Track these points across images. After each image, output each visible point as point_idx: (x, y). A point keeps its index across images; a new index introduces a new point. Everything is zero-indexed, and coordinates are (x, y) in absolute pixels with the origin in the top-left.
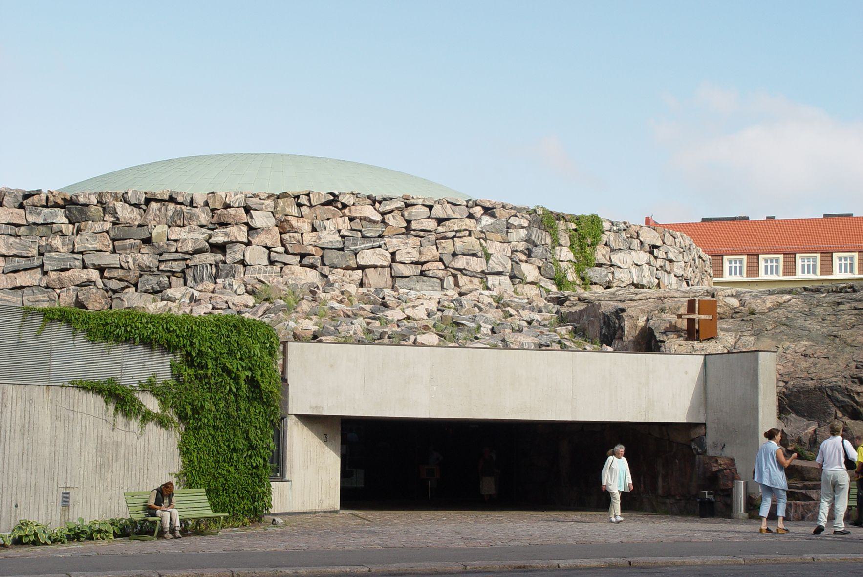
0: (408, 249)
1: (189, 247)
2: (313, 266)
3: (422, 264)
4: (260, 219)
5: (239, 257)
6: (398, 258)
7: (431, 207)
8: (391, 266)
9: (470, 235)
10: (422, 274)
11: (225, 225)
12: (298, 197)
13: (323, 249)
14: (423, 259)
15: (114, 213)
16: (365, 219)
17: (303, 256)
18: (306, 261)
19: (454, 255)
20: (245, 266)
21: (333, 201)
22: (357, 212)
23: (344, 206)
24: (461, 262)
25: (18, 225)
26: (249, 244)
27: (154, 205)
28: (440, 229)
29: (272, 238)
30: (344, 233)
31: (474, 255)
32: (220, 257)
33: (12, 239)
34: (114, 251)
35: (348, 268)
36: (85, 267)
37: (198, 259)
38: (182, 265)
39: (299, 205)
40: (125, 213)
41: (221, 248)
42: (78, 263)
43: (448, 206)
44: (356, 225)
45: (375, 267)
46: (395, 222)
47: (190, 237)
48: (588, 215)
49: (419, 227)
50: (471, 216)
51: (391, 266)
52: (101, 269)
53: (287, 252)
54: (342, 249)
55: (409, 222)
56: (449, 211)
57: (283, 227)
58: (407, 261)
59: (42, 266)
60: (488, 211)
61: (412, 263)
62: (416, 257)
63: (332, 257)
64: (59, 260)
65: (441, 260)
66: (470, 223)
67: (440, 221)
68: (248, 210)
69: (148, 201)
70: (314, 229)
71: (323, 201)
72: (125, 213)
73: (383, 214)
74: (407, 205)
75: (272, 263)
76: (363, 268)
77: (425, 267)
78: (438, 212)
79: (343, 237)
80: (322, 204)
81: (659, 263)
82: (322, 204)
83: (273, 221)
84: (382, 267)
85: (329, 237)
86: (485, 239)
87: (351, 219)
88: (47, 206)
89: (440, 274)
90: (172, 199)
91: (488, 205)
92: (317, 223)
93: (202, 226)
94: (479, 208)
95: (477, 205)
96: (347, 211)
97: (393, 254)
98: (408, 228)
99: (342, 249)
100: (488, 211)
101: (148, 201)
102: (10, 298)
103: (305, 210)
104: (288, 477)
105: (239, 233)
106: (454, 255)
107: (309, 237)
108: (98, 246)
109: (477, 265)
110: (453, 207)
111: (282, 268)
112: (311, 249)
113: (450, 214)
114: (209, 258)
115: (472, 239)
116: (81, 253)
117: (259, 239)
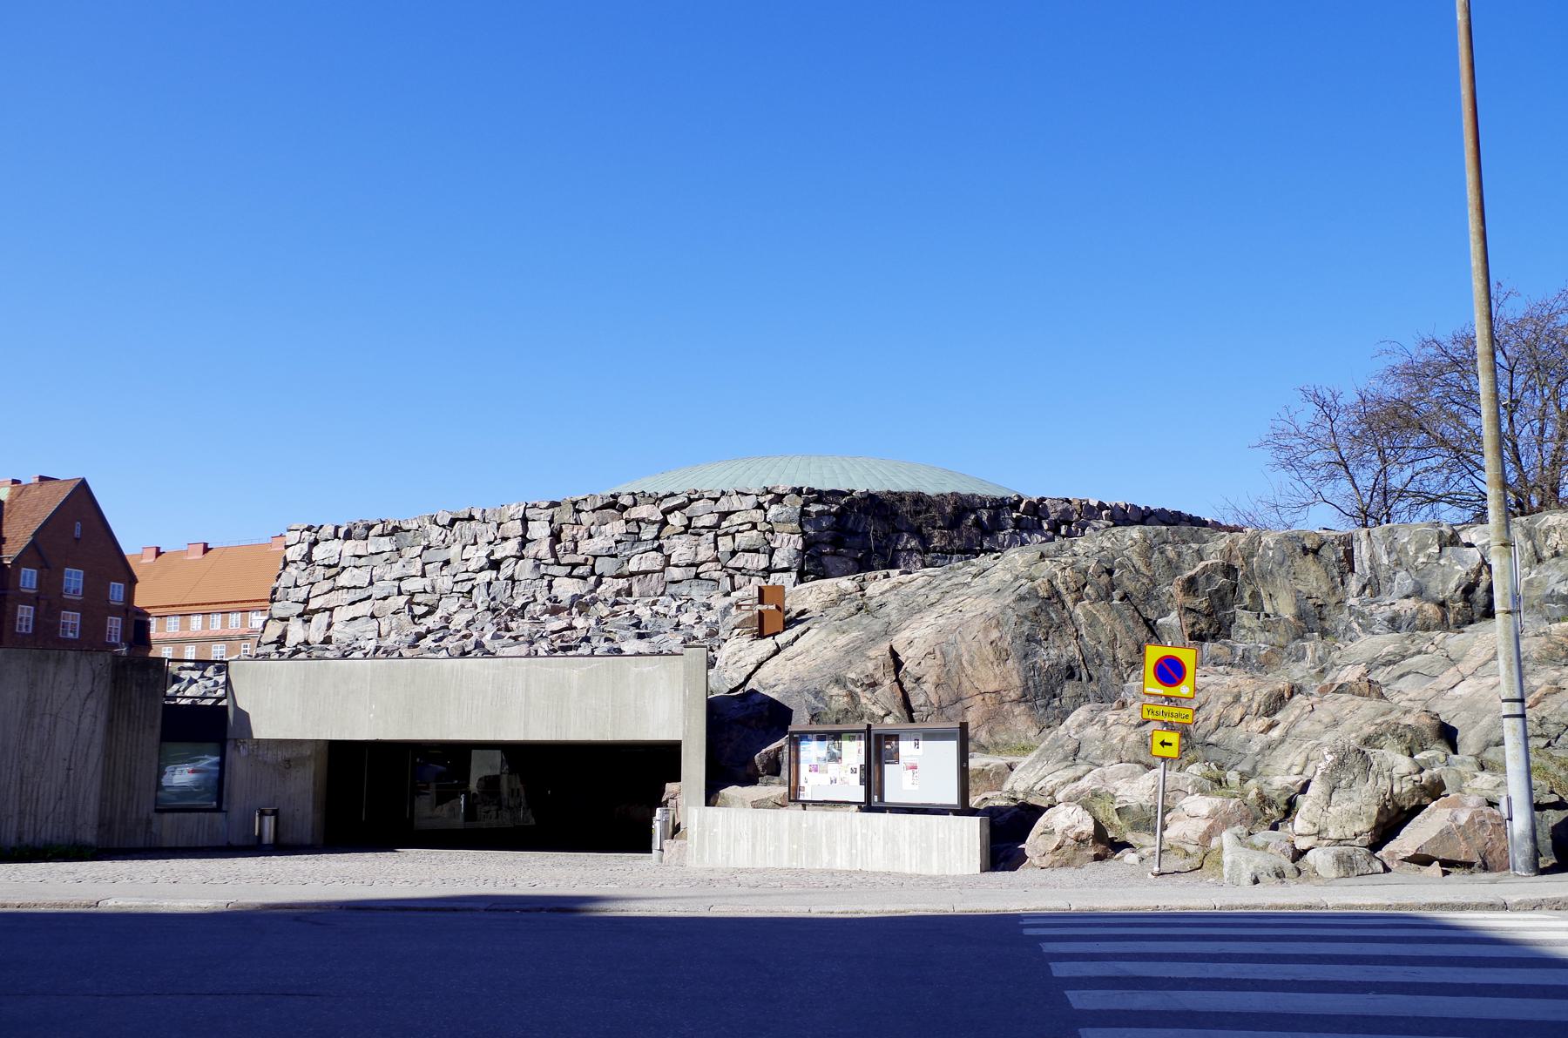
0: (680, 549)
1: (473, 566)
3: (697, 566)
6: (673, 560)
7: (716, 500)
8: (663, 571)
10: (697, 576)
11: (505, 539)
12: (575, 504)
13: (595, 557)
14: (700, 558)
15: (426, 537)
16: (643, 520)
17: (574, 566)
18: (575, 573)
19: (734, 553)
20: (514, 582)
21: (613, 504)
22: (635, 513)
23: (625, 508)
24: (740, 561)
25: (360, 557)
26: (522, 557)
28: (724, 524)
29: (544, 550)
31: (757, 551)
34: (424, 575)
35: (617, 577)
36: (400, 593)
38: (467, 586)
39: (578, 511)
41: (495, 565)
43: (735, 497)
44: (633, 528)
45: (646, 573)
46: (676, 520)
47: (478, 556)
48: (931, 490)
49: (700, 524)
50: (760, 506)
51: (663, 571)
54: (615, 556)
55: (690, 519)
56: (735, 502)
57: (556, 537)
58: (683, 563)
60: (779, 499)
61: (688, 565)
62: (689, 557)
65: (717, 560)
66: (757, 515)
67: (724, 515)
68: (525, 520)
69: (453, 522)
70: (590, 536)
71: (599, 504)
72: (435, 534)
73: (666, 512)
74: (691, 501)
75: (542, 577)
76: (632, 574)
78: (723, 505)
79: (617, 542)
80: (601, 508)
82: (601, 508)
83: (548, 532)
84: (654, 572)
85: (598, 544)
86: (772, 532)
87: (627, 522)
88: (382, 535)
89: (716, 575)
90: (471, 518)
92: (593, 528)
93: (490, 543)
94: (770, 497)
95: (768, 492)
96: (625, 515)
98: (687, 527)
99: (615, 556)
100: (779, 499)
101: (453, 522)
102: (347, 630)
103: (583, 515)
104: (224, 807)
105: (511, 547)
106: (734, 553)
110: (743, 498)
111: (550, 583)
112: (580, 559)
113: (736, 505)
116: (400, 579)
117: (531, 550)
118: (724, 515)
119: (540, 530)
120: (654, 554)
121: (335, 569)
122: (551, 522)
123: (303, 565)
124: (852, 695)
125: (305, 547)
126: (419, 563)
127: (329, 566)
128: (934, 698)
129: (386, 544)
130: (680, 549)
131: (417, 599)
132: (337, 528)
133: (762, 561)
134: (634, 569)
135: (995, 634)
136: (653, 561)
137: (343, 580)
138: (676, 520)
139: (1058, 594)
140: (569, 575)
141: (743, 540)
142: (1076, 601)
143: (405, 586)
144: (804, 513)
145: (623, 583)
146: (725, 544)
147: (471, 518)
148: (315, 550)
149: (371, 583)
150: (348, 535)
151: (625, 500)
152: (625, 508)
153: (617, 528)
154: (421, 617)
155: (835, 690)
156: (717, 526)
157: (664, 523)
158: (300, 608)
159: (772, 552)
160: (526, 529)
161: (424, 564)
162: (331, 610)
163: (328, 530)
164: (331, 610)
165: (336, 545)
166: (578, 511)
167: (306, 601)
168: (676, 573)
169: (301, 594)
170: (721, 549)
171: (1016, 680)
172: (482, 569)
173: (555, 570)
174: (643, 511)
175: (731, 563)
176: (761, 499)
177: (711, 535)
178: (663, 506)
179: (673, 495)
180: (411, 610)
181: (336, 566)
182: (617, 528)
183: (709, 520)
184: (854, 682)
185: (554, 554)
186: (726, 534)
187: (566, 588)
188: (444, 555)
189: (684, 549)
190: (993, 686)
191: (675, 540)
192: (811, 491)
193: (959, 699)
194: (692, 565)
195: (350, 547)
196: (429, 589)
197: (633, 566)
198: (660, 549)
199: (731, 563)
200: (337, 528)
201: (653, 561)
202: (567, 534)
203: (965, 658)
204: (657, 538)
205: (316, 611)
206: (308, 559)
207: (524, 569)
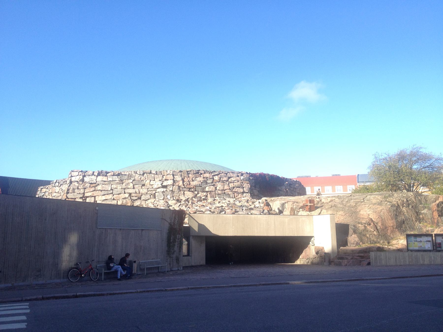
0: (219, 186)
2: (192, 192)
4: (178, 178)
5: (171, 189)
6: (218, 188)
7: (227, 174)
9: (238, 182)
10: (225, 193)
12: (187, 172)
14: (225, 188)
17: (190, 188)
18: (190, 190)
19: (234, 188)
23: (201, 174)
24: (236, 190)
25: (105, 181)
27: (145, 174)
28: (230, 180)
29: (181, 183)
30: (202, 182)
32: (165, 189)
33: (103, 186)
34: (134, 188)
36: (125, 193)
37: (158, 190)
38: (154, 192)
40: (137, 177)
41: (165, 187)
42: (123, 192)
45: (211, 191)
49: (223, 180)
50: (238, 176)
52: (130, 194)
53: (185, 187)
55: (220, 178)
56: (232, 175)
58: (220, 189)
59: (112, 193)
60: (242, 175)
62: (222, 188)
63: (199, 189)
64: (117, 191)
65: (230, 189)
66: (238, 178)
68: (173, 175)
69: (143, 174)
70: (193, 181)
76: (207, 192)
77: (226, 191)
81: (292, 189)
87: (204, 178)
89: (230, 193)
90: (151, 173)
91: (243, 173)
92: (194, 179)
93: (160, 180)
96: (202, 176)
97: (216, 188)
101: (143, 174)
103: (190, 175)
104: (190, 255)
105: (170, 182)
107: (191, 183)
108: (129, 187)
109: (241, 190)
112: (192, 187)
113: (232, 175)
114: (162, 190)
115: (239, 183)
116: (124, 189)
118: (229, 178)
119: (178, 178)
120: (212, 187)
121: (94, 185)
122: (181, 176)
123: (81, 183)
124: (365, 226)
125: (81, 177)
126: (131, 185)
127: (91, 184)
128: (382, 227)
129: (116, 178)
130: (219, 186)
131: (133, 195)
132: (93, 172)
133: (241, 190)
134: (208, 190)
135: (390, 214)
136: (212, 188)
137: (99, 188)
138: (216, 178)
139: (398, 205)
140: (189, 191)
141: (236, 184)
142: (403, 207)
143: (127, 191)
144: (249, 179)
145: (205, 194)
146: (231, 185)
147: (151, 173)
148: (85, 178)
149: (111, 189)
150: (99, 174)
151: (202, 172)
152: (201, 174)
153: (200, 179)
154: (134, 200)
155: (360, 225)
156: (228, 180)
157: (213, 178)
158: (82, 196)
159: (243, 188)
160: (174, 177)
161: (134, 185)
162: (95, 197)
163: (91, 173)
164: (95, 197)
165: (94, 177)
166: (188, 174)
167: (84, 193)
168: (220, 192)
169: (82, 191)
170: (231, 186)
171: (395, 224)
172: (159, 188)
173: (185, 189)
174: (207, 175)
175: (234, 190)
176: (239, 174)
177: (228, 183)
178: (213, 175)
179: (215, 171)
180: (131, 198)
181: (95, 183)
182: (200, 179)
183: (225, 179)
184: (365, 223)
185: (184, 185)
186: (231, 183)
187: (189, 195)
188: (143, 183)
189: (220, 186)
190: (392, 225)
191: (217, 183)
192: (250, 173)
193: (386, 228)
194: (223, 190)
195: (100, 178)
196: (138, 192)
197: (207, 189)
198: (214, 185)
199: (234, 190)
200: (93, 172)
201: (212, 188)
202: (186, 179)
203: (386, 219)
204: (212, 183)
205: (88, 197)
206: (83, 180)
207: (176, 188)
